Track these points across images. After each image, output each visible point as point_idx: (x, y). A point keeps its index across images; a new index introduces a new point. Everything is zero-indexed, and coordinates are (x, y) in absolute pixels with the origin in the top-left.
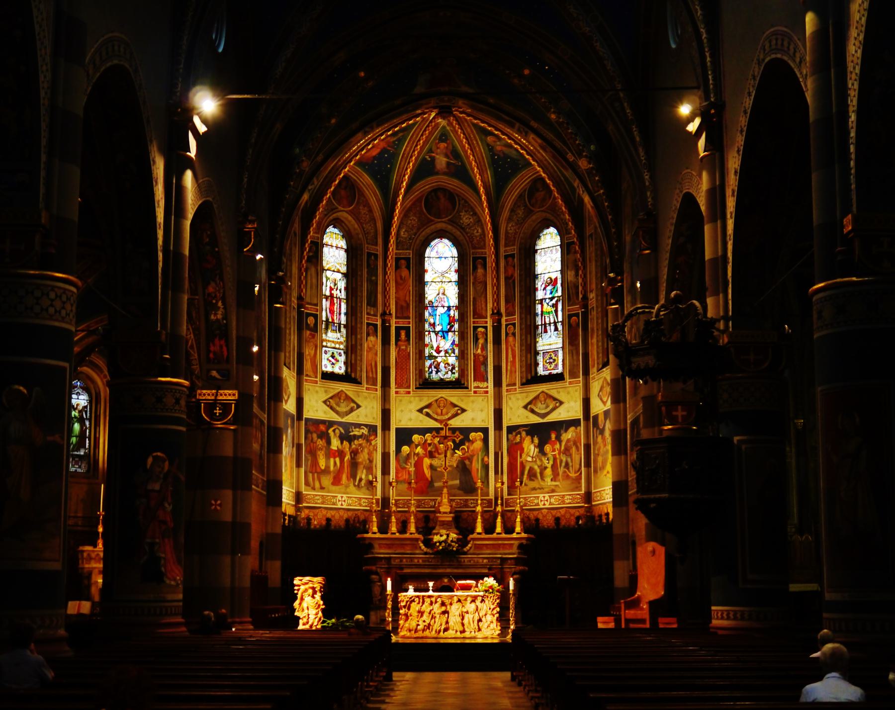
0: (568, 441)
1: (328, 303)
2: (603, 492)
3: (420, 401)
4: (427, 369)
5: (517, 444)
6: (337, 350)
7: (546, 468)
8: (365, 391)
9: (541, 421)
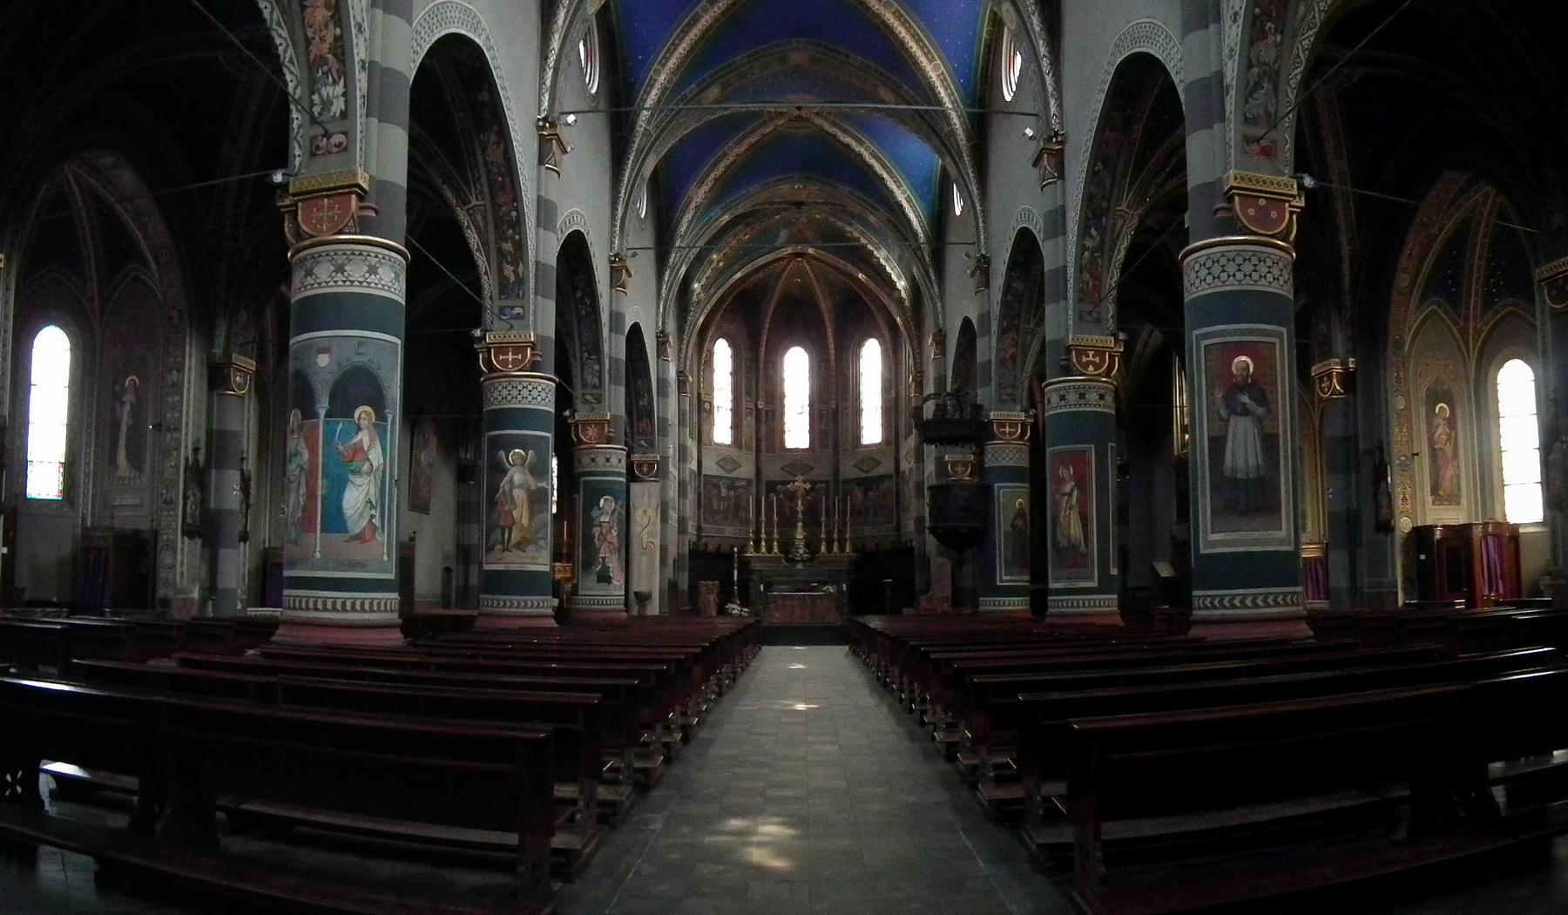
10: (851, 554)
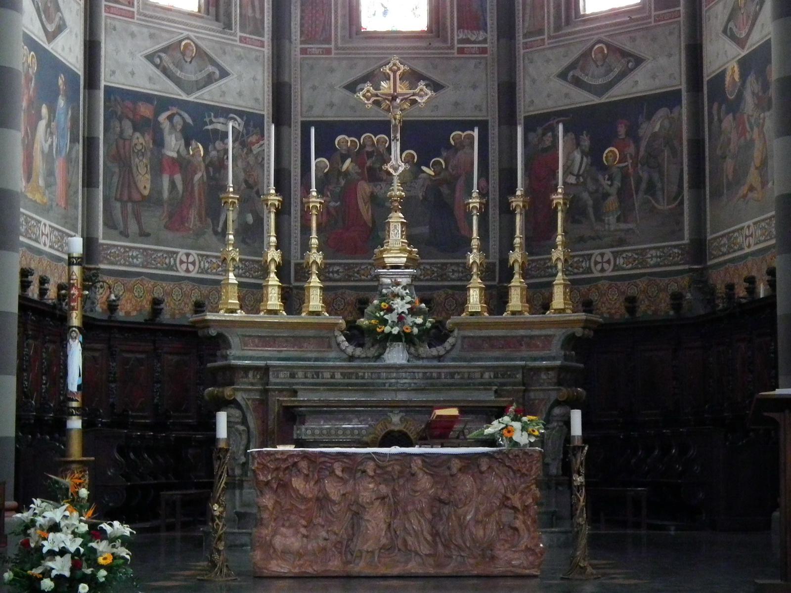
0: (655, 136)
2: (736, 234)
3: (351, 68)
5: (545, 150)
7: (606, 195)
8: (238, 43)
9: (596, 100)
10: (570, 316)
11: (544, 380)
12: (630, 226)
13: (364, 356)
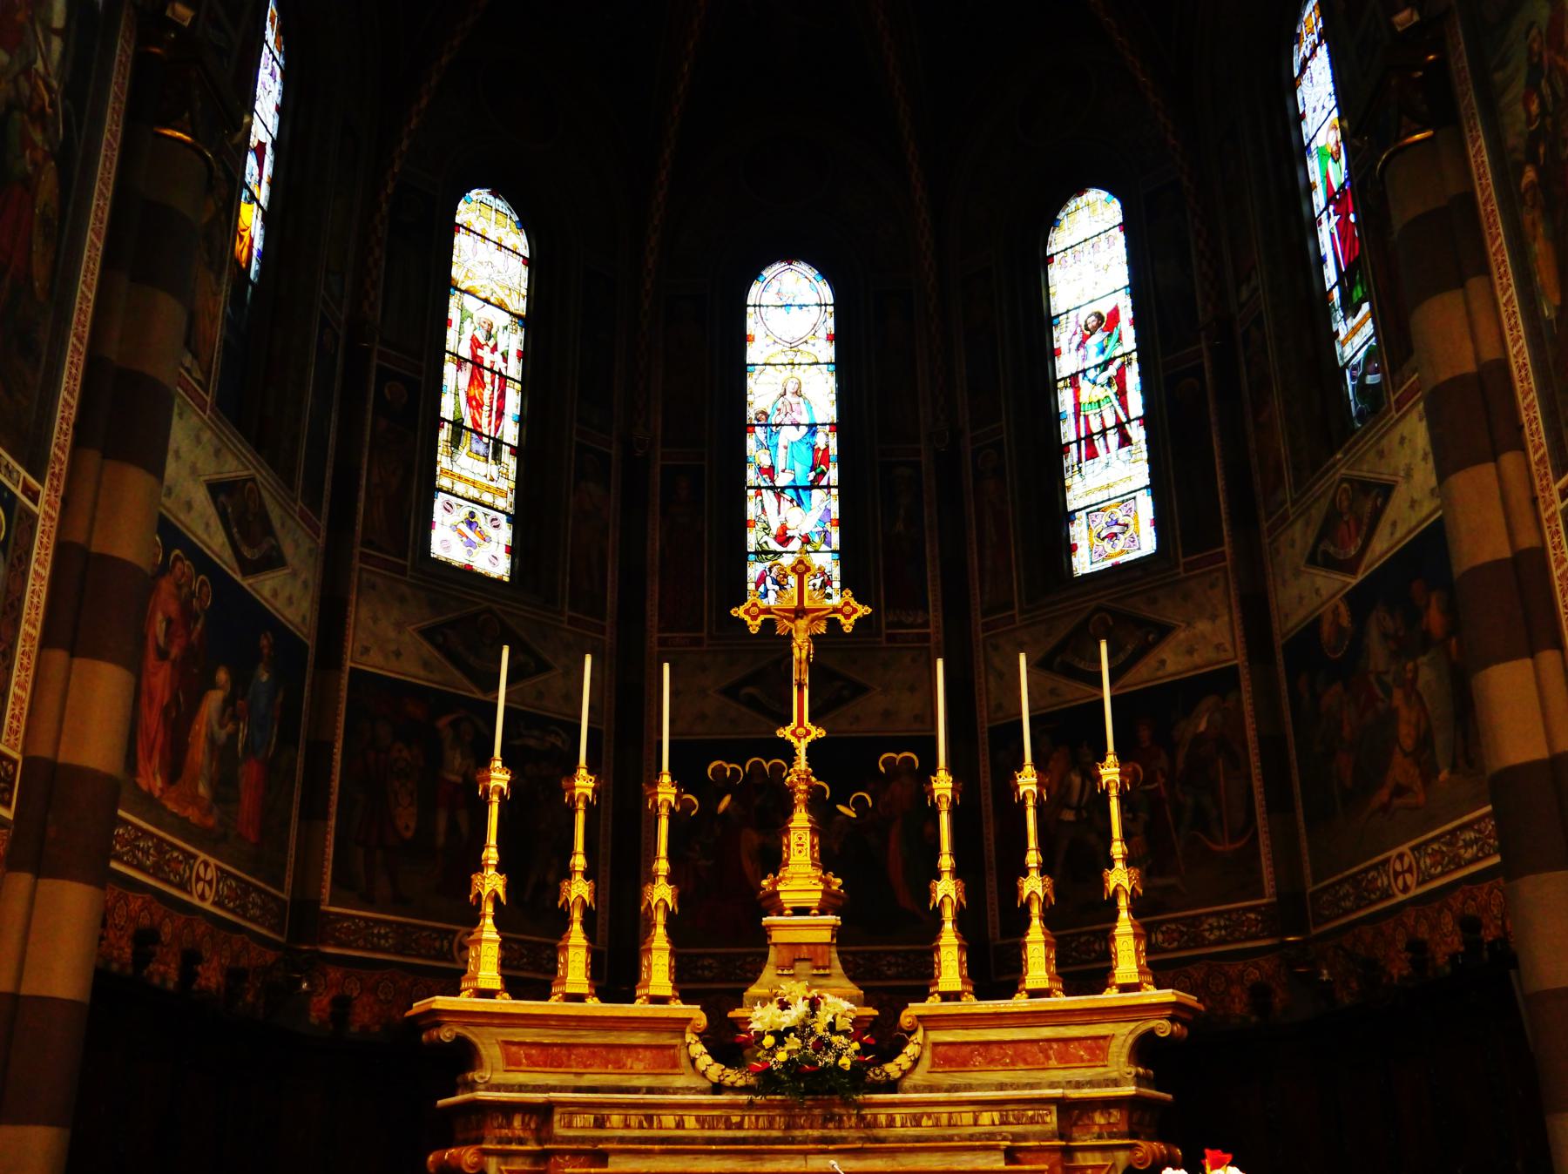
1: (464, 377)
4: (751, 586)
6: (486, 510)
8: (566, 626)
11: (1101, 1126)
12: (1172, 881)
13: (740, 1083)
